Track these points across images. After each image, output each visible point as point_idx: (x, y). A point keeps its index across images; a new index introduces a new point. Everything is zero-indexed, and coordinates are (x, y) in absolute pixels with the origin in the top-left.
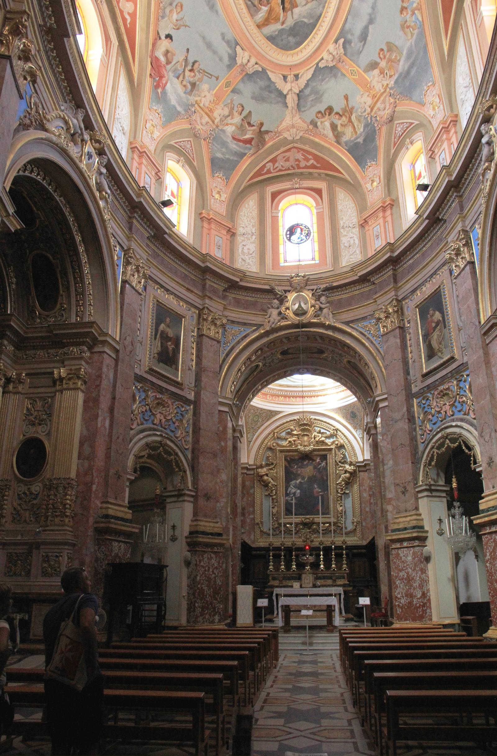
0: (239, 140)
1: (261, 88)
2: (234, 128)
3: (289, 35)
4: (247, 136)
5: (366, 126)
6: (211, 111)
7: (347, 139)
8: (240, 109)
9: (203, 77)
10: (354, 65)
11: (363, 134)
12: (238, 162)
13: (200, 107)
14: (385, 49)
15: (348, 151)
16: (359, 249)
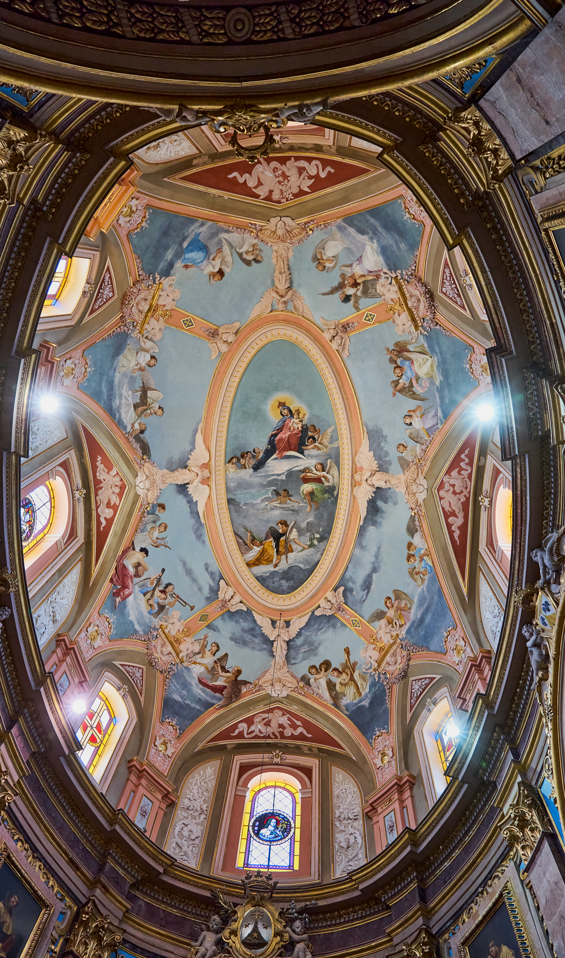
0: (208, 686)
1: (243, 630)
2: (202, 669)
3: (282, 578)
4: (220, 683)
5: (373, 685)
6: (178, 641)
7: (348, 701)
8: (215, 649)
9: (175, 602)
10: (357, 615)
11: (369, 696)
12: (200, 713)
13: (164, 632)
14: (393, 598)
15: (348, 716)
16: (363, 851)
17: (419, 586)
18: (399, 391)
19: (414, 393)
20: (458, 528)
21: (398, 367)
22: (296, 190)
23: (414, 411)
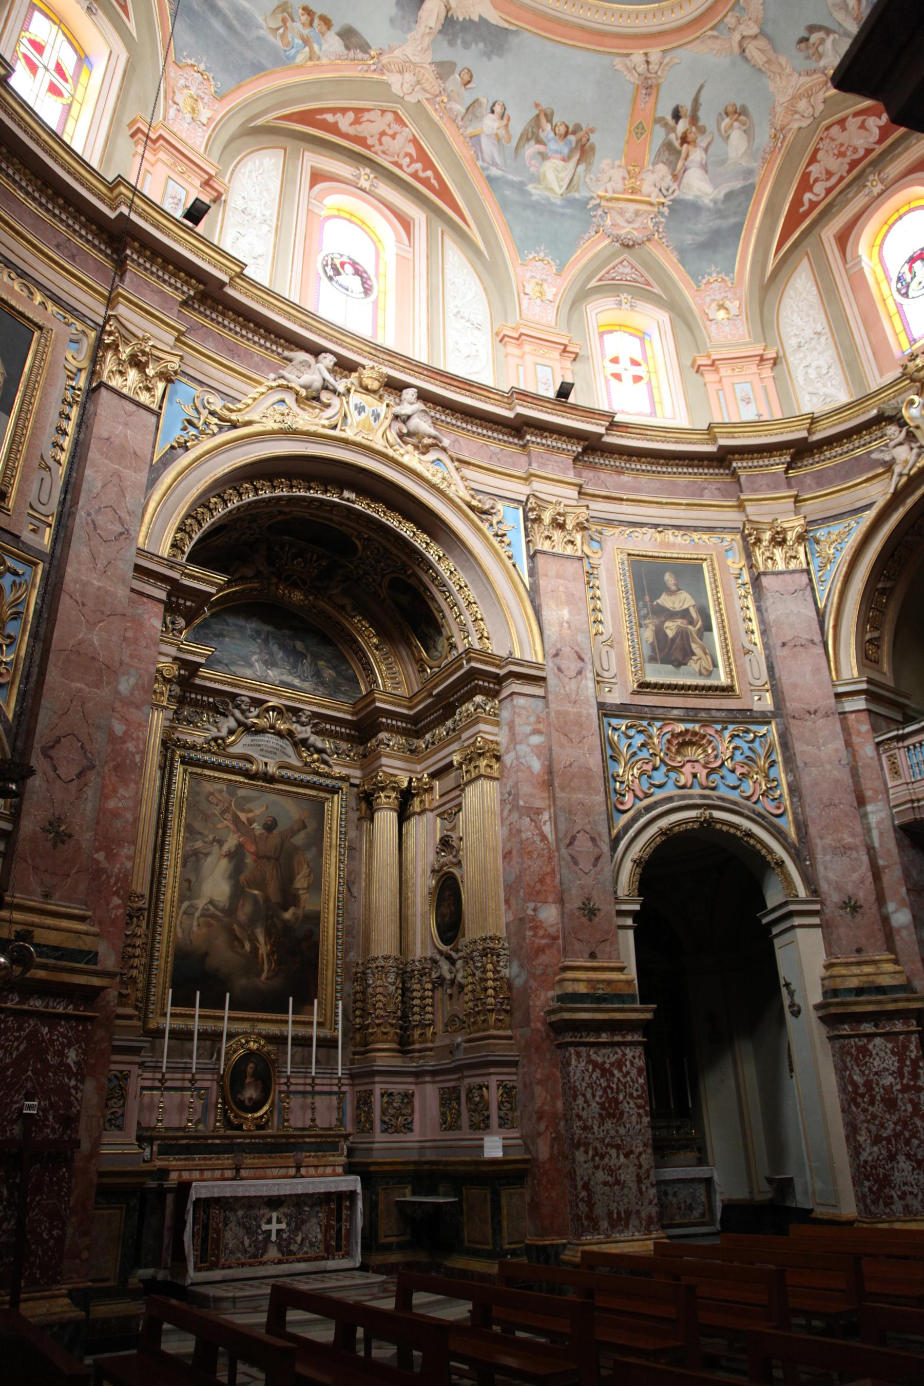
17: (265, 20)
18: (538, 116)
19: (528, 140)
20: (336, 123)
21: (567, 133)
22: (820, 155)
23: (507, 126)
